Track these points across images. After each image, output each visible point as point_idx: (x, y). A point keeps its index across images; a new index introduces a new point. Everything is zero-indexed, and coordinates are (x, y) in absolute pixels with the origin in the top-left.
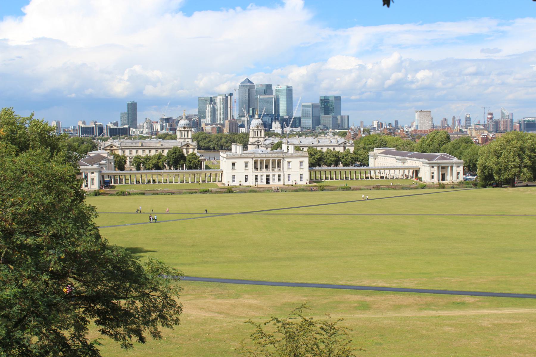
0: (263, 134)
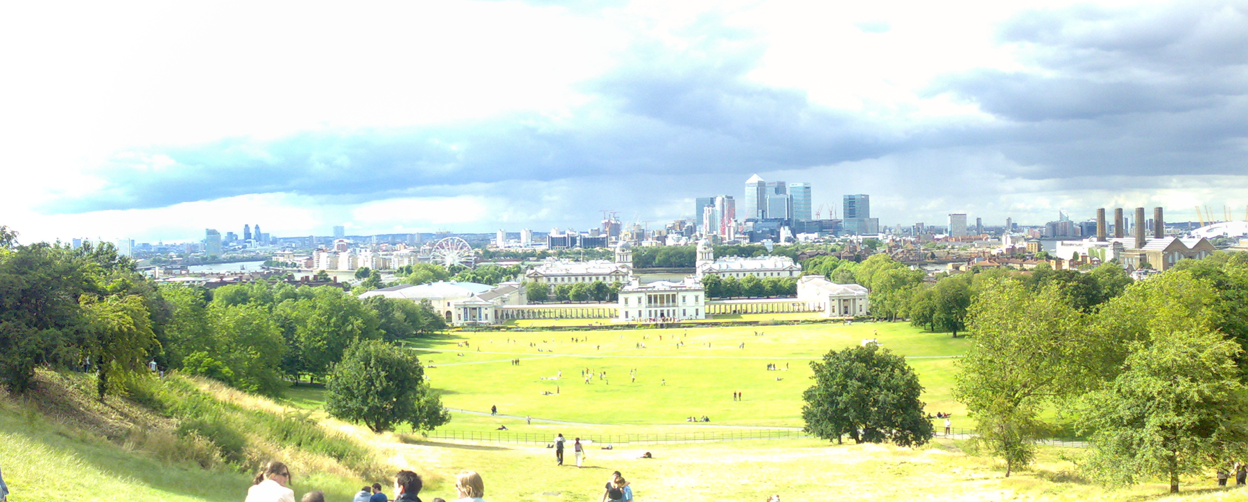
0: (711, 255)
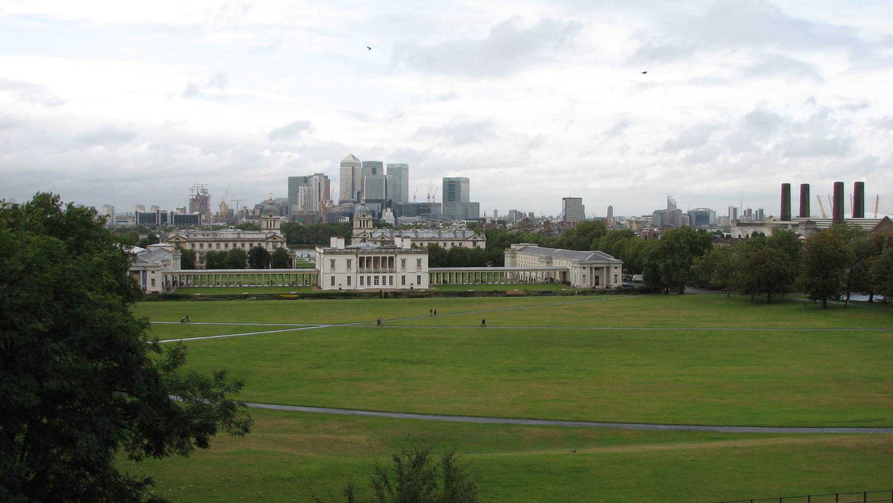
0: (370, 224)
